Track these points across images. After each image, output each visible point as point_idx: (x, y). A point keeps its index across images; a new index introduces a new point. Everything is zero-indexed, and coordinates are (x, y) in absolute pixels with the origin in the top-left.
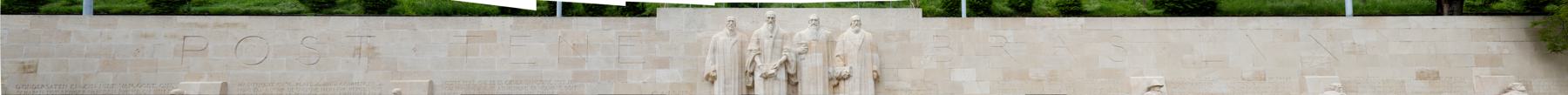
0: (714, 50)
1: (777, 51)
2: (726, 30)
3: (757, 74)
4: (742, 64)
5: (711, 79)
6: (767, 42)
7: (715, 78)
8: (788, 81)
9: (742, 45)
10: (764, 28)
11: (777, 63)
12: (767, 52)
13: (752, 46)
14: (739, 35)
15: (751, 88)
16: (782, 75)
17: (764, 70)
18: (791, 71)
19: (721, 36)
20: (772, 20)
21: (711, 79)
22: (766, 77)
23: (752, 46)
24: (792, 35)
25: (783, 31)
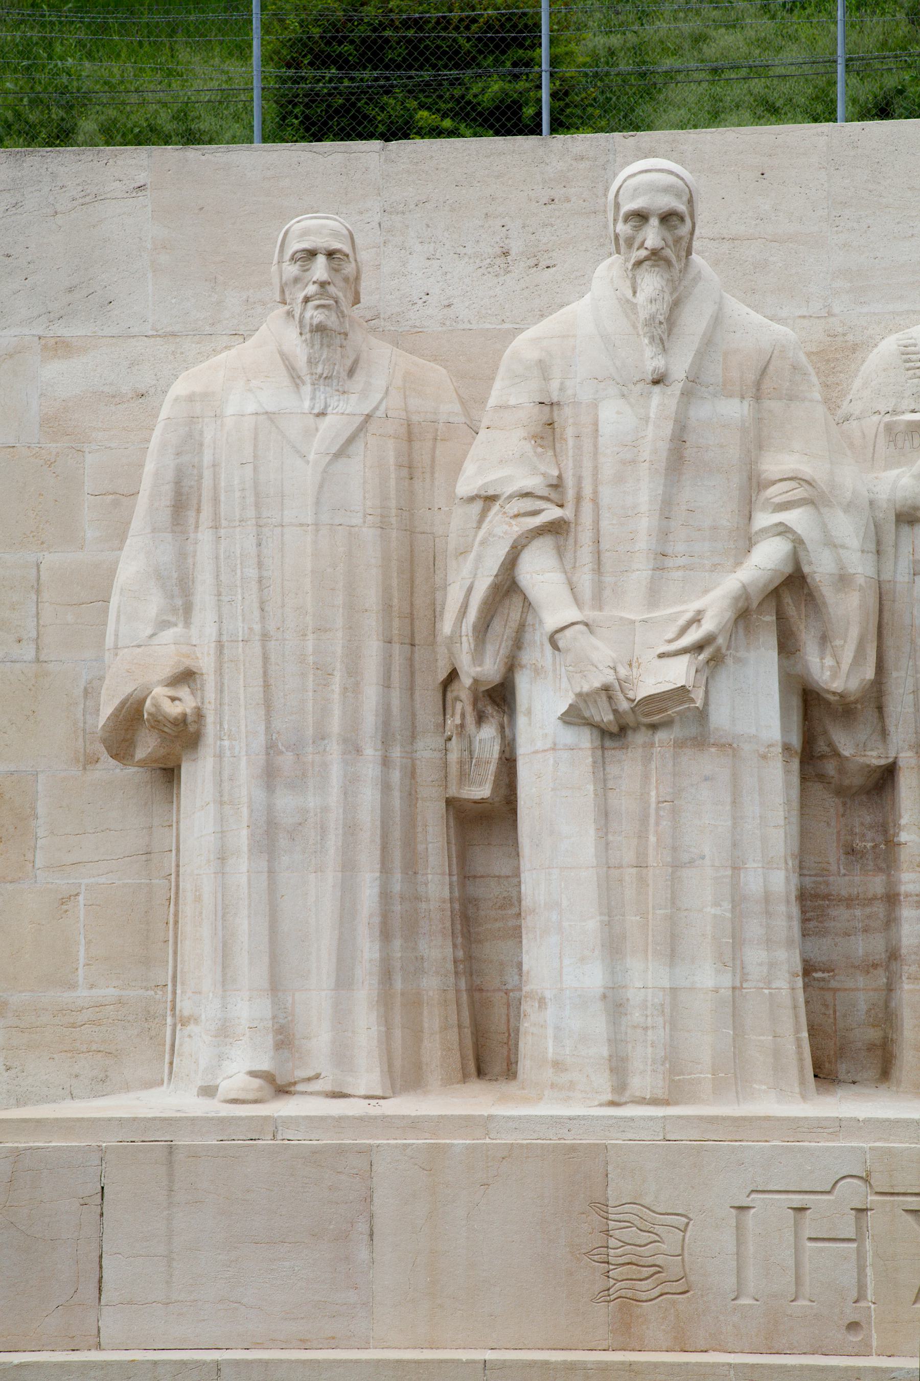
0: (182, 505)
1: (712, 499)
2: (280, 334)
3: (542, 704)
4: (411, 621)
5: (157, 747)
6: (623, 426)
7: (185, 735)
8: (811, 758)
9: (417, 452)
10: (593, 309)
11: (712, 601)
12: (628, 505)
13: (498, 460)
14: (385, 363)
15: (487, 821)
16: (753, 704)
17: (599, 660)
18: (836, 669)
19: (240, 383)
20: (667, 236)
21: (157, 747)
22: (615, 725)
23: (498, 460)
24: (836, 357)
25: (759, 327)
